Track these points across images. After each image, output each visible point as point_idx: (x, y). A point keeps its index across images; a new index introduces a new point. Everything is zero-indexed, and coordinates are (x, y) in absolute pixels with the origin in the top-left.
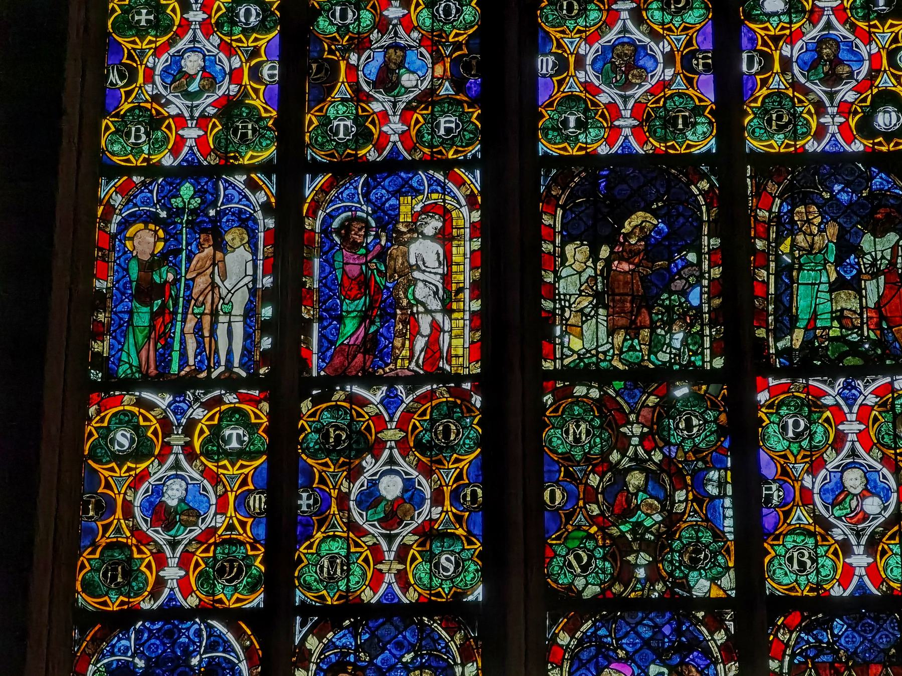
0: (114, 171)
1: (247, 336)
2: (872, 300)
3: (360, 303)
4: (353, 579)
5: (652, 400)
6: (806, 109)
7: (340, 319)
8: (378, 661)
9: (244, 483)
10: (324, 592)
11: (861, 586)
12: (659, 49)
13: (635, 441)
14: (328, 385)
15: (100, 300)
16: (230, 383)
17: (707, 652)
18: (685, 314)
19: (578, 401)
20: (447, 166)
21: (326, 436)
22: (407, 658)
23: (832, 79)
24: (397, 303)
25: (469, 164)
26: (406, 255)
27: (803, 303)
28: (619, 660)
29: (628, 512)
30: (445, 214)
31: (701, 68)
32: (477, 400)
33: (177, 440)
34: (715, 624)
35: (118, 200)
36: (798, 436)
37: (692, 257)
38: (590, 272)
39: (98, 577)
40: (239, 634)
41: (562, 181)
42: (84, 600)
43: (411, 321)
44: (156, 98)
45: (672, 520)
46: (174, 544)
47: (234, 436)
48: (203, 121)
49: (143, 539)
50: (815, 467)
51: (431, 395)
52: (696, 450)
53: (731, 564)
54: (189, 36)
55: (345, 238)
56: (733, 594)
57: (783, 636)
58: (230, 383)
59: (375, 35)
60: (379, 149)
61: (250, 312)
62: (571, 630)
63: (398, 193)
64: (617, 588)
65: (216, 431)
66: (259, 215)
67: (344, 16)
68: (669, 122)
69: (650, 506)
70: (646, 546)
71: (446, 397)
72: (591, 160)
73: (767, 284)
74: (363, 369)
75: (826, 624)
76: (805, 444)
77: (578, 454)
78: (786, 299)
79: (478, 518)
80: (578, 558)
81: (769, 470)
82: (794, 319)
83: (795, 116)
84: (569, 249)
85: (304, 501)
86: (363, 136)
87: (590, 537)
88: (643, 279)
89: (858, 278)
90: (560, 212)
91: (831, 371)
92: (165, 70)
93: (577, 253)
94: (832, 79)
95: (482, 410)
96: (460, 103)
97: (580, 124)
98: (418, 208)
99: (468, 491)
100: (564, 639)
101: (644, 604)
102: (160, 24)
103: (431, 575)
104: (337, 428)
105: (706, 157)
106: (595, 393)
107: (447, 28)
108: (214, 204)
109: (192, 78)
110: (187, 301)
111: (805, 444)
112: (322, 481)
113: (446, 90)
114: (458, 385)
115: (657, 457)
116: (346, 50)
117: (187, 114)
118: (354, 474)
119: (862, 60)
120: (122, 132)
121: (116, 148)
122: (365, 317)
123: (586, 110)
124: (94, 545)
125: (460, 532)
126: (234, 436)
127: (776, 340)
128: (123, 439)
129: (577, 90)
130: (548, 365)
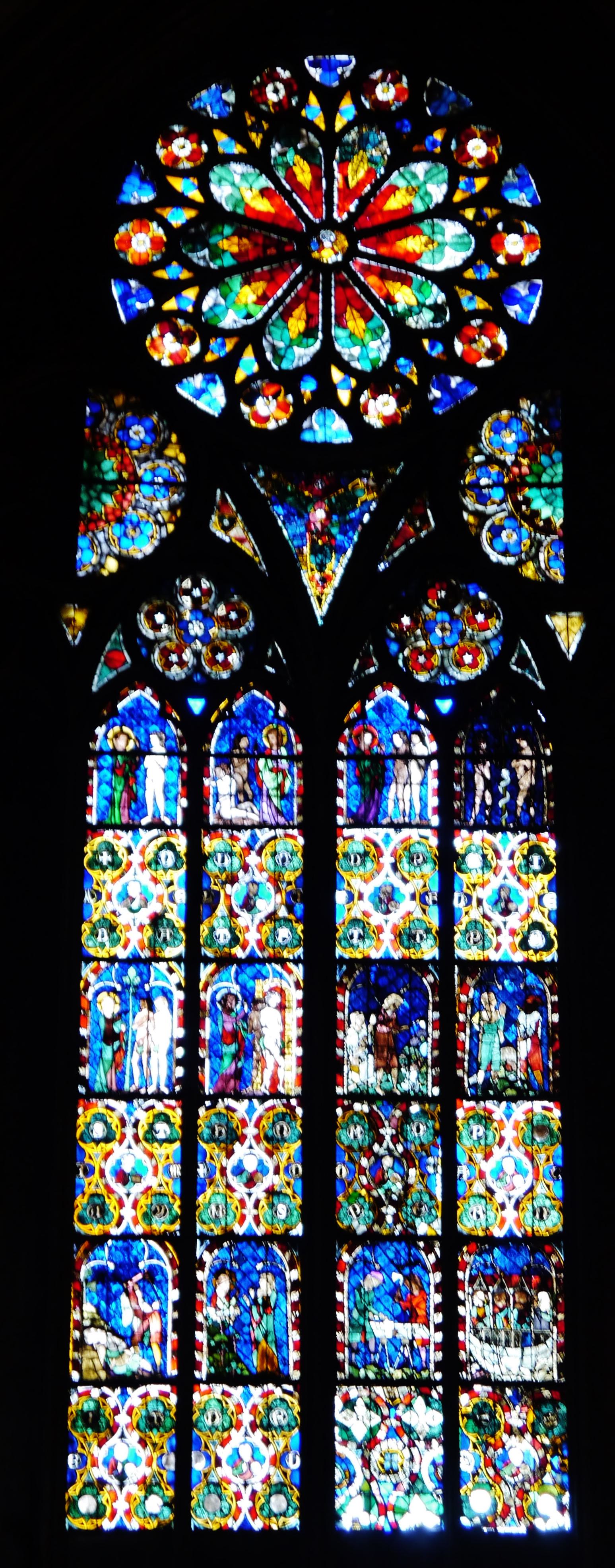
0: (90, 959)
1: (170, 1068)
2: (523, 1054)
3: (233, 1048)
4: (229, 1219)
5: (398, 1113)
6: (490, 931)
7: (221, 1058)
8: (244, 1268)
9: (168, 1158)
10: (212, 1226)
11: (510, 1231)
12: (406, 890)
13: (388, 1138)
14: (214, 1099)
15: (83, 1042)
16: (159, 1096)
17: (424, 1267)
18: (418, 1059)
19: (356, 1113)
20: (282, 962)
21: (213, 1130)
22: (260, 1266)
23: (506, 912)
24: (253, 1048)
25: (296, 962)
26: (258, 1019)
27: (484, 1055)
28: (375, 1270)
29: (383, 1181)
30: (282, 992)
31: (431, 903)
32: (299, 1111)
33: (129, 1131)
34: (429, 1250)
35: (92, 978)
36: (479, 1138)
37: (422, 1024)
38: (364, 1032)
39: (86, 1214)
40: (166, 1249)
41: (349, 973)
42: (79, 1227)
43: (261, 1060)
44: (114, 913)
45: (407, 1187)
46: (128, 1195)
47: (162, 1130)
48: (141, 928)
49: (110, 1191)
50: (488, 1156)
51: (273, 1107)
52: (422, 1145)
53: (439, 1214)
54: (132, 870)
55: (224, 1006)
56: (440, 1233)
57: (466, 1258)
58: (159, 1096)
59: (241, 874)
60: (244, 948)
61: (170, 1052)
62: (350, 1252)
63: (254, 978)
64: (376, 1228)
65: (151, 1127)
66: (174, 989)
67: (223, 861)
68: (412, 937)
69: (396, 1179)
70: (392, 1202)
71: (281, 1109)
72: (367, 961)
73: (464, 1043)
74: (235, 1089)
75: (490, 1252)
76: (482, 1142)
77: (355, 1146)
78: (475, 1052)
79: (299, 1184)
80: (355, 1209)
81: (462, 1157)
82: (479, 1065)
83: (484, 935)
84: (353, 1016)
85: (202, 1171)
86: (235, 941)
87: (360, 1196)
88: (395, 1037)
89: (516, 1041)
90: (347, 993)
91: (499, 1097)
92: (119, 895)
93: (357, 1018)
94: (506, 912)
95: (303, 1118)
96: (290, 921)
97: (361, 937)
98: (266, 989)
99: (294, 1168)
100: (346, 1257)
101: (391, 1238)
102: (115, 864)
103: (273, 1217)
104: (220, 1125)
105: (433, 961)
106: (366, 1108)
107: (283, 871)
108: (148, 982)
109: (133, 900)
110: (133, 1044)
111: (482, 1142)
112: (212, 1158)
113: (283, 912)
114: (288, 1101)
115: (400, 1148)
116: (224, 883)
117: (132, 924)
118: (230, 1154)
119: (522, 900)
120: (94, 934)
121: (90, 943)
122: (236, 1057)
123: (364, 928)
124: (84, 1193)
125: (289, 1191)
126: (162, 1130)
127: (469, 1077)
128: (99, 1130)
129: (360, 916)
130: (339, 1090)
